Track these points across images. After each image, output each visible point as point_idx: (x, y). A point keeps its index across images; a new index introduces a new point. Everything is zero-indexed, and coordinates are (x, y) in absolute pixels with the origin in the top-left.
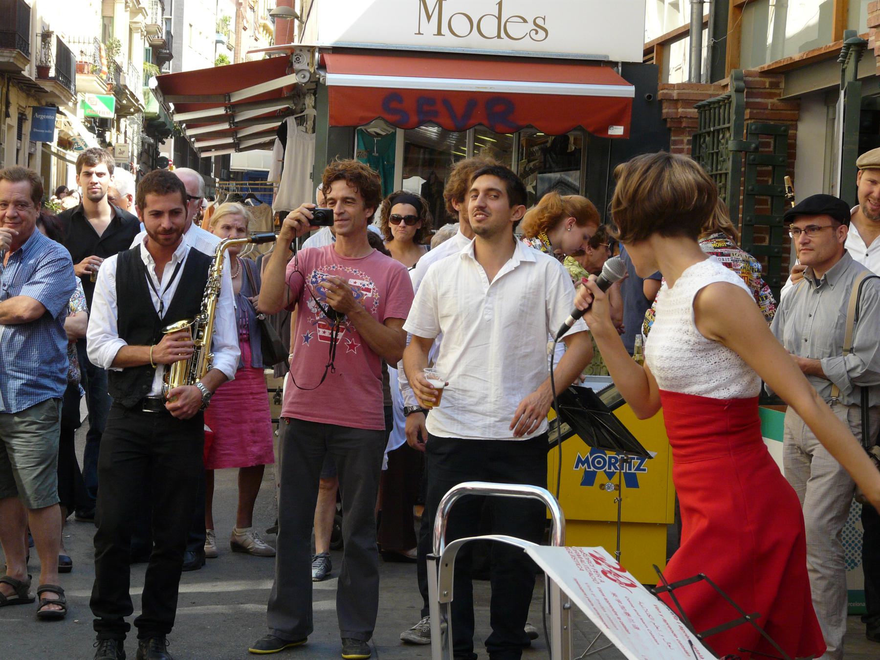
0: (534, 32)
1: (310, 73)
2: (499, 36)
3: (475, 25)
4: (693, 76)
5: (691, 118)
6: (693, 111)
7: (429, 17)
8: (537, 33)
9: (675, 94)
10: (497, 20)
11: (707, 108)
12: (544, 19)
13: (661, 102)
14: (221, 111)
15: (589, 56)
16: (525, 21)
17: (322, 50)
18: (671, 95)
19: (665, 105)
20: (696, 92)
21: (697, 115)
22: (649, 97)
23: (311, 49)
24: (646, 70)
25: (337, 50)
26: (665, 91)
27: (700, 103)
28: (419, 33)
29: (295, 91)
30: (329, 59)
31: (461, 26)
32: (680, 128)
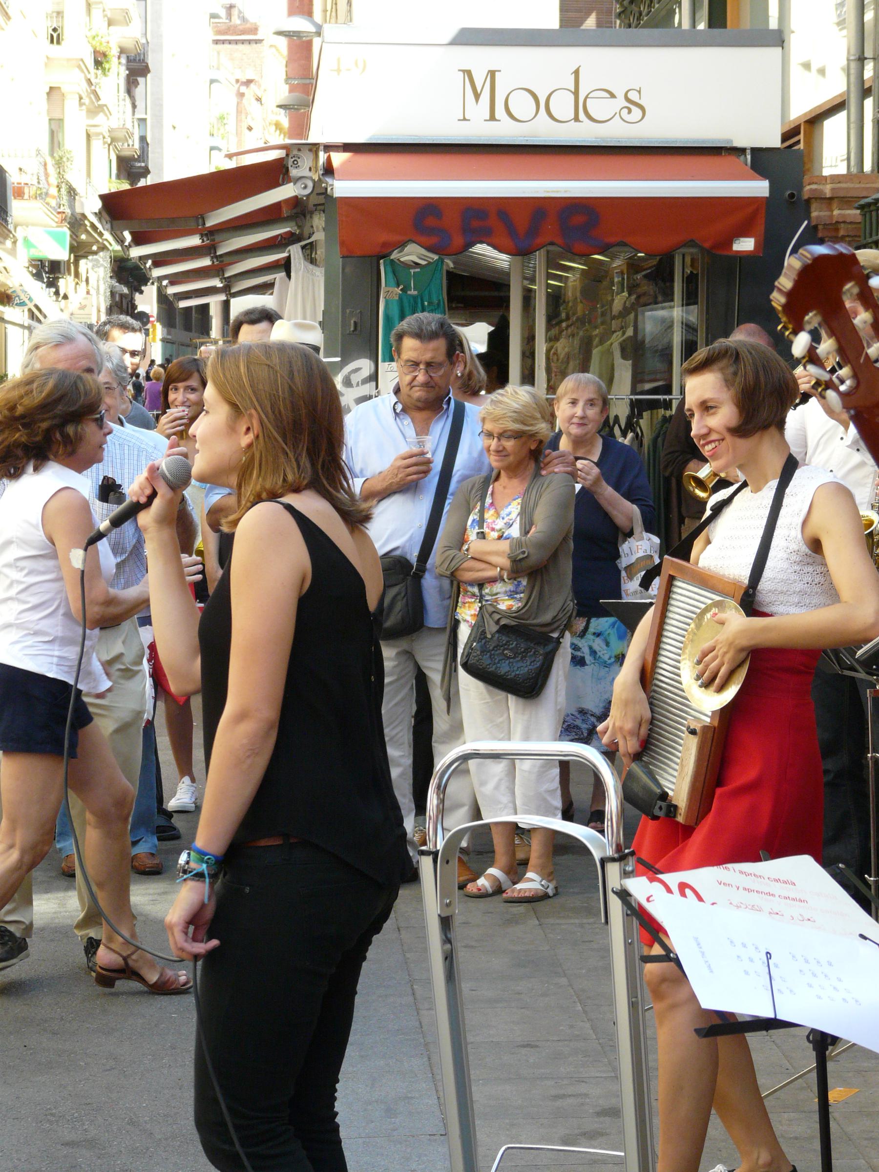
0: (626, 111)
1: (314, 181)
2: (576, 119)
3: (543, 105)
4: (852, 163)
5: (851, 223)
6: (854, 214)
7: (477, 96)
8: (630, 111)
9: (827, 190)
10: (572, 97)
11: (873, 208)
12: (639, 92)
13: (808, 202)
14: (195, 241)
15: (704, 141)
16: (613, 96)
17: (328, 148)
18: (821, 191)
19: (814, 205)
20: (858, 186)
21: (859, 219)
22: (792, 196)
23: (314, 148)
24: (787, 159)
25: (347, 147)
26: (814, 187)
27: (863, 202)
28: (465, 119)
29: (297, 209)
30: (338, 159)
31: (522, 106)
32: (837, 237)
